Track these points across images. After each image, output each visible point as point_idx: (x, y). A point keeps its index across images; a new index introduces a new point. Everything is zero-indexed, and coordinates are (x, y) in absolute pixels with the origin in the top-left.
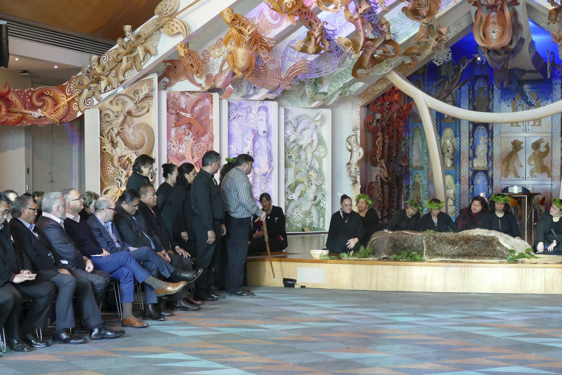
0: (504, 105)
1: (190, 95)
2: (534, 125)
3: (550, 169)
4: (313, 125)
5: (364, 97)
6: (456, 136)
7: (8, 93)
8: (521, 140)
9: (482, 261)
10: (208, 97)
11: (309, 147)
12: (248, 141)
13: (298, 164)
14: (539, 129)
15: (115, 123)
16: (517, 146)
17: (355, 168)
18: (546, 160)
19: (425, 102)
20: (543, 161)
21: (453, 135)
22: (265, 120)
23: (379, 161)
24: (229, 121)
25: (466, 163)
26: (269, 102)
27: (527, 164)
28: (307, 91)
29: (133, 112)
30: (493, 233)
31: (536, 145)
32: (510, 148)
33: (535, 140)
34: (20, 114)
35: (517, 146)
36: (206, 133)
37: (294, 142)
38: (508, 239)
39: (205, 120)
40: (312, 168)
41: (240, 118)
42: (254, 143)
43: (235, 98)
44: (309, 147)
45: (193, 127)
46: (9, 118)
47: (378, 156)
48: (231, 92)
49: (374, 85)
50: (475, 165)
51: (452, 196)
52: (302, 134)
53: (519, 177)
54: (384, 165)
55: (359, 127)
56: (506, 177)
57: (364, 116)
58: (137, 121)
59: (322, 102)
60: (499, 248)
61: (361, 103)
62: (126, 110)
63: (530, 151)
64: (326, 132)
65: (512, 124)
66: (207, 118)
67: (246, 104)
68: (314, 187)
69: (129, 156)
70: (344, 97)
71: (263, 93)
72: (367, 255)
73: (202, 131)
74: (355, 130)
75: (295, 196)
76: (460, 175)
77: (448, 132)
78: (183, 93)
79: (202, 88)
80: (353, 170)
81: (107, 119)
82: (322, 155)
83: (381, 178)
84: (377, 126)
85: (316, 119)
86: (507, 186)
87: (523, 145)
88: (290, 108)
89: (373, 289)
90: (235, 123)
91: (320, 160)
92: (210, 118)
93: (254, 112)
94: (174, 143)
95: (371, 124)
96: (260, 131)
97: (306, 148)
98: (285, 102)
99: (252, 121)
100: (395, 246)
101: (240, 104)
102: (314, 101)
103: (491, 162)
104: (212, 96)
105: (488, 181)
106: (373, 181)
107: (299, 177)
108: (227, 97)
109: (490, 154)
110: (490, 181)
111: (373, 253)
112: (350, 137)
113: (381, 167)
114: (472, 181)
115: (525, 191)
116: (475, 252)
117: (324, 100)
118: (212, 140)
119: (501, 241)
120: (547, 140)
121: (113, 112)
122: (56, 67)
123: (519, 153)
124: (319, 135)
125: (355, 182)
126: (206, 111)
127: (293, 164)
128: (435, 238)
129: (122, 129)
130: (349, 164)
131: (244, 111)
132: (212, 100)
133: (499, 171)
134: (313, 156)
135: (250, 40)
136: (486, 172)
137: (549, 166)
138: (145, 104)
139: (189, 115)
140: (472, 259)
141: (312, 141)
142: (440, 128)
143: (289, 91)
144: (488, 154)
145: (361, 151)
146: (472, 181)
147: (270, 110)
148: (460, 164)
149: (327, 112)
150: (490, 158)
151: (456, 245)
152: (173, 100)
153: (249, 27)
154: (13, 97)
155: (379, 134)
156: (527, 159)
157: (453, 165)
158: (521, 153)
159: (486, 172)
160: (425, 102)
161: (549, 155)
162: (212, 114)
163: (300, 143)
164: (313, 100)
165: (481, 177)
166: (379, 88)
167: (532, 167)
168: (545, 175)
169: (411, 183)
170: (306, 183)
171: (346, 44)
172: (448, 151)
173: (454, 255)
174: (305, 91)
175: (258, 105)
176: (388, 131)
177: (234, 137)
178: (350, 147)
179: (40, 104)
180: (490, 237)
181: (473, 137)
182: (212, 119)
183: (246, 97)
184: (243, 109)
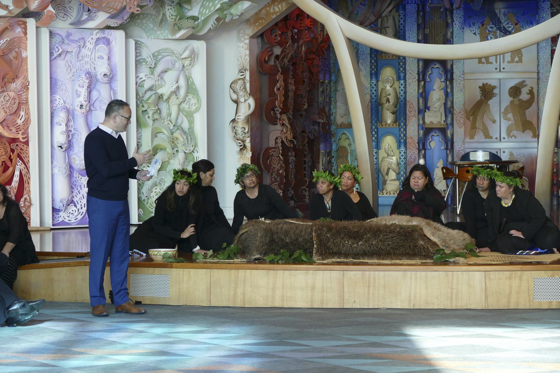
0: (468, 33)
2: (512, 61)
3: (536, 126)
4: (178, 65)
5: (256, 21)
6: (399, 79)
8: (493, 83)
9: (398, 261)
10: (19, 25)
11: (174, 97)
12: (80, 89)
13: (157, 122)
14: (519, 67)
16: (487, 92)
17: (242, 127)
18: (530, 113)
19: (340, 29)
20: (525, 115)
21: (395, 77)
22: (106, 57)
23: (279, 116)
24: (51, 61)
25: (414, 118)
26: (112, 31)
27: (502, 119)
28: (168, 14)
30: (416, 222)
31: (515, 91)
32: (478, 95)
33: (513, 83)
35: (487, 92)
36: (17, 77)
37: (150, 89)
38: (439, 230)
39: (16, 58)
40: (178, 127)
41: (69, 56)
42: (90, 93)
43: (62, 26)
44: (174, 97)
47: (278, 110)
48: (51, 18)
49: (269, 5)
50: (428, 120)
51: (394, 166)
52: (162, 78)
53: (491, 138)
54: (286, 122)
55: (248, 67)
56: (472, 137)
57: (256, 51)
59: (190, 31)
60: (422, 243)
61: (250, 31)
63: (507, 100)
65: (480, 60)
66: (18, 55)
67: (76, 35)
68: (181, 156)
70: (223, 25)
71: (101, 18)
72: (232, 255)
76: (405, 135)
77: (388, 73)
79: (10, 12)
80: (240, 131)
82: (193, 108)
83: (282, 142)
84: (275, 66)
85: (183, 57)
86: (467, 151)
87: (496, 91)
88: (144, 39)
89: (239, 304)
90: (61, 63)
91: (190, 116)
92: (24, 55)
93: (90, 45)
95: (266, 62)
96: (98, 74)
97: (169, 98)
98: (136, 31)
99: (87, 59)
100: (272, 241)
101: (69, 35)
102: (180, 29)
103: (450, 116)
104: (25, 23)
105: (446, 143)
106: (271, 146)
108: (46, 25)
109: (449, 103)
110: (449, 144)
111: (243, 252)
113: (283, 125)
114: (423, 145)
115: (494, 158)
116: (388, 248)
117: (193, 28)
118: (26, 87)
119: (428, 232)
120: (531, 83)
123: (490, 102)
124: (188, 79)
125: (243, 148)
126: (16, 45)
127: (150, 122)
128: (330, 229)
130: (233, 121)
131: (74, 45)
132: (25, 28)
133: (463, 129)
134: (179, 110)
136: (443, 131)
137: (535, 122)
140: (383, 259)
141: (178, 88)
142: (376, 66)
143: (138, 15)
144: (445, 104)
145: (251, 101)
146: (423, 145)
147: (114, 43)
148: (405, 119)
149: (200, 46)
150: (449, 110)
151: (360, 240)
155: (279, 77)
156: (502, 111)
157: (395, 121)
158: (493, 103)
159: (443, 131)
160: (340, 29)
161: (534, 105)
162: (26, 49)
163: (160, 91)
164: (177, 27)
165: (436, 138)
166: (277, 9)
167: (510, 123)
168: (529, 133)
169: (334, 147)
170: (169, 150)
172: (388, 100)
173: (358, 254)
174: (164, 15)
175: (96, 35)
176: (292, 73)
177: (59, 83)
178: (234, 97)
180: (408, 227)
181: (424, 79)
182: (27, 57)
183: (77, 23)
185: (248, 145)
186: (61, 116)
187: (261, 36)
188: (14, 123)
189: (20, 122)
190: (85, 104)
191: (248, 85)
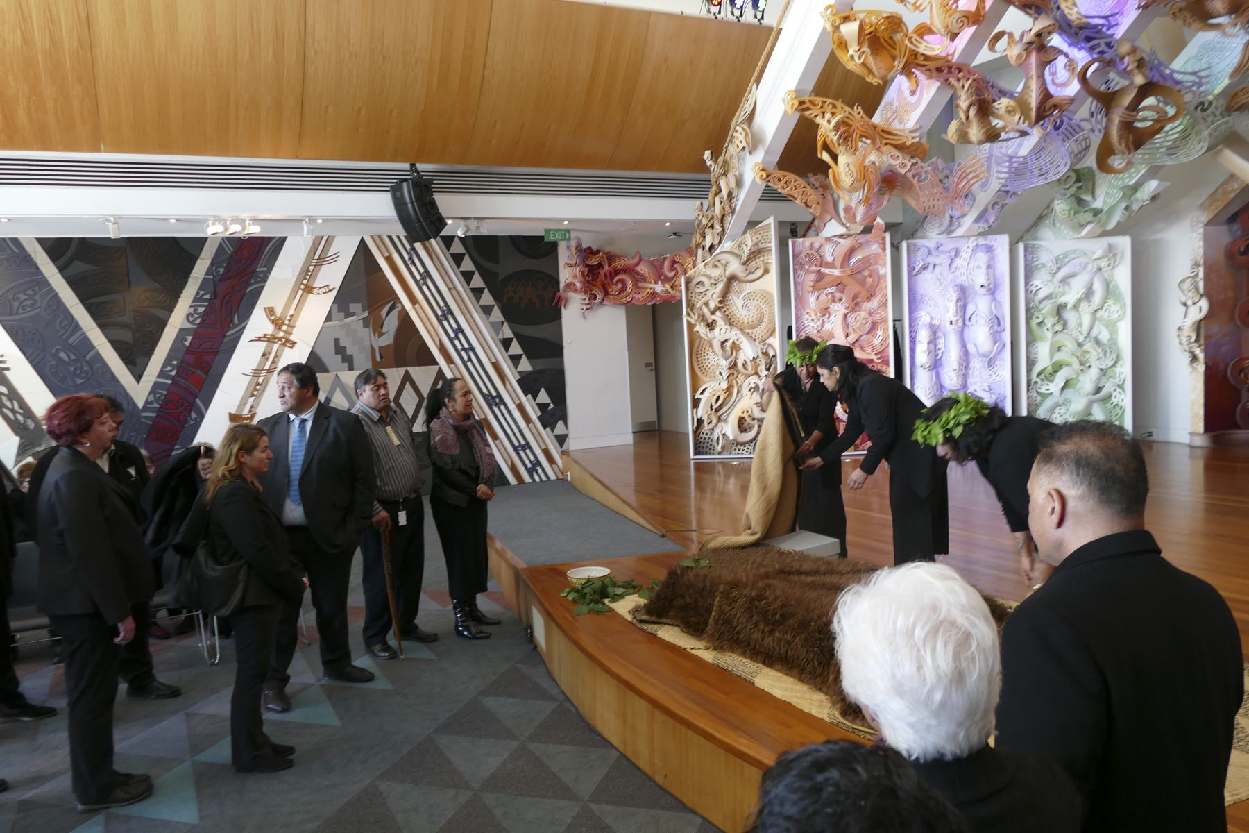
1: (842, 241)
4: (1091, 267)
7: (638, 264)
13: (1059, 335)
15: (709, 293)
22: (984, 266)
29: (741, 275)
41: (938, 269)
44: (1084, 305)
55: (1202, 262)
58: (749, 288)
61: (1204, 218)
62: (728, 273)
64: (1123, 277)
67: (949, 245)
68: (1094, 373)
73: (864, 294)
74: (1197, 265)
75: (1055, 387)
78: (828, 239)
81: (702, 289)
91: (1112, 326)
93: (965, 254)
94: (813, 316)
97: (1076, 307)
107: (1059, 357)
112: (1183, 281)
121: (709, 277)
125: (1194, 358)
127: (1049, 334)
129: (720, 302)
135: (846, 139)
138: (758, 262)
139: (836, 272)
145: (1204, 304)
153: (828, 116)
154: (643, 269)
163: (1063, 300)
170: (1076, 365)
171: (1009, 112)
178: (1183, 299)
179: (671, 274)
183: (949, 231)
184: (943, 252)
185: (1201, 356)
186: (923, 336)
187: (1232, 220)
188: (870, 343)
189: (876, 342)
190: (954, 319)
191: (1201, 285)
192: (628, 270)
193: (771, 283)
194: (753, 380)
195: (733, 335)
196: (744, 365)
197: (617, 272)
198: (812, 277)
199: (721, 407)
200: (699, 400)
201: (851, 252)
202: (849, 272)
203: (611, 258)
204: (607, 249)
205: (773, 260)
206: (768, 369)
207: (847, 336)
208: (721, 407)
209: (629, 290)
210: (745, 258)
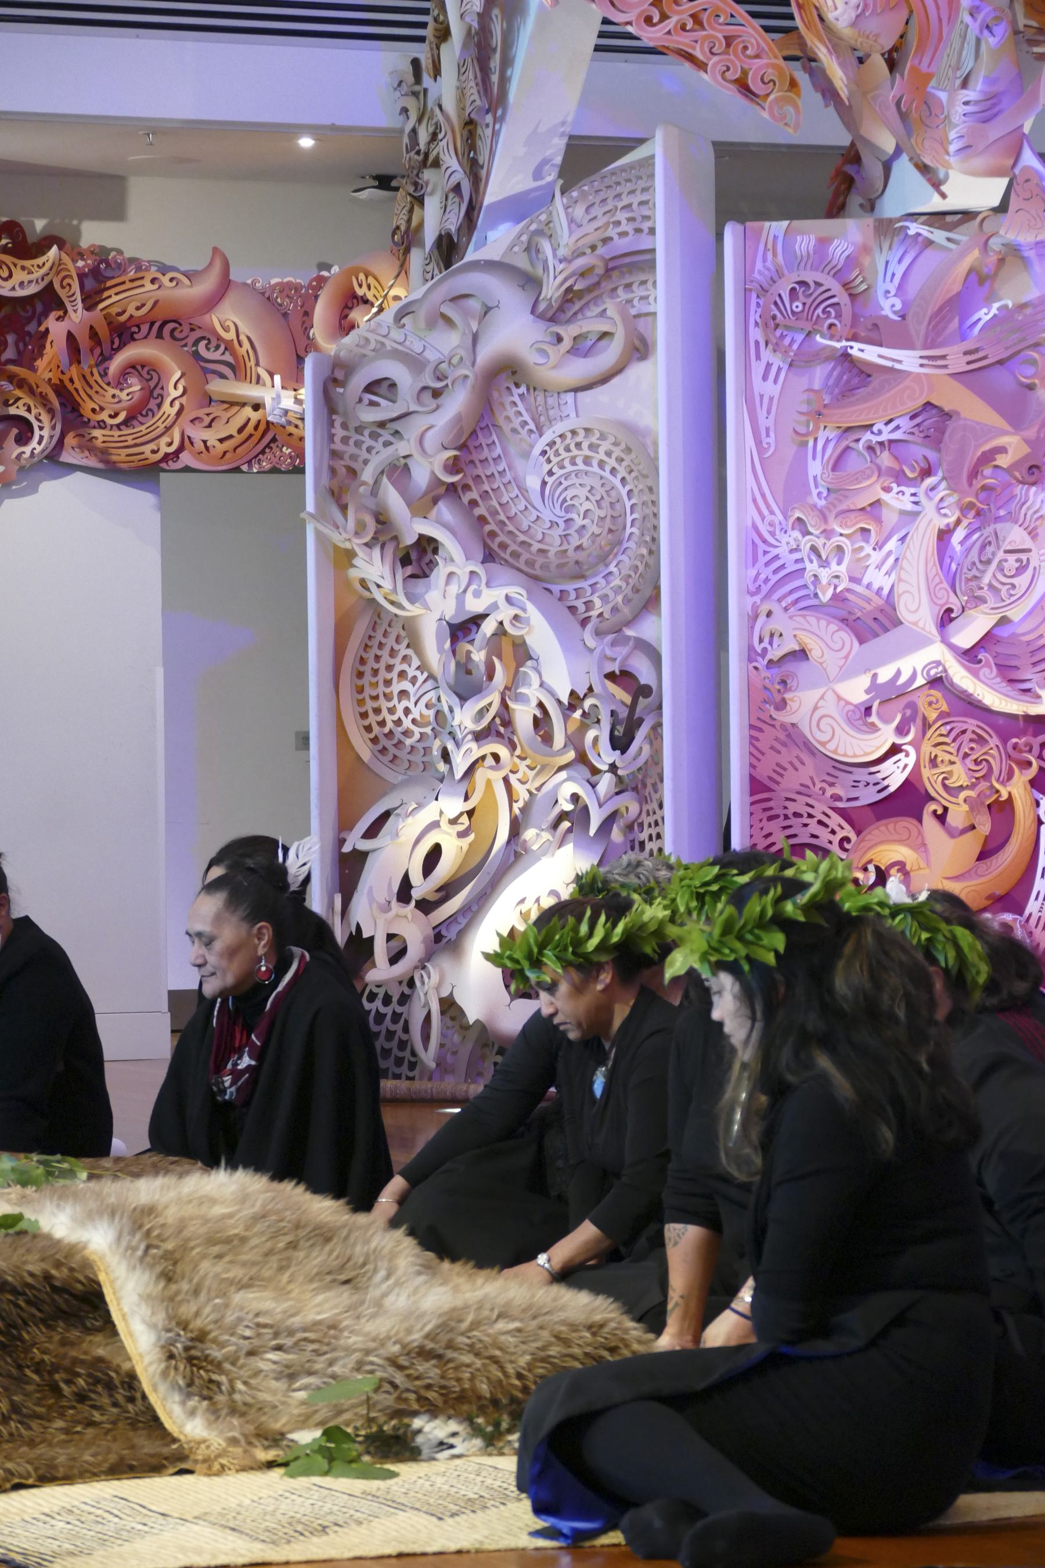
1: (939, 236)
34: (248, 411)
45: (951, 425)
46: (198, 434)
62: (486, 353)
69: (505, 614)
81: (386, 410)
122: (306, 142)
129: (453, 466)
152: (809, 277)
192: (167, 325)
193: (651, 397)
194: (567, 787)
195: (497, 598)
196: (541, 722)
197: (124, 332)
198: (819, 375)
199: (447, 890)
200: (359, 858)
201: (981, 282)
202: (958, 362)
203: (100, 275)
204: (94, 234)
205: (663, 299)
206: (620, 743)
207: (946, 619)
208: (447, 890)
209: (169, 410)
210: (551, 290)
